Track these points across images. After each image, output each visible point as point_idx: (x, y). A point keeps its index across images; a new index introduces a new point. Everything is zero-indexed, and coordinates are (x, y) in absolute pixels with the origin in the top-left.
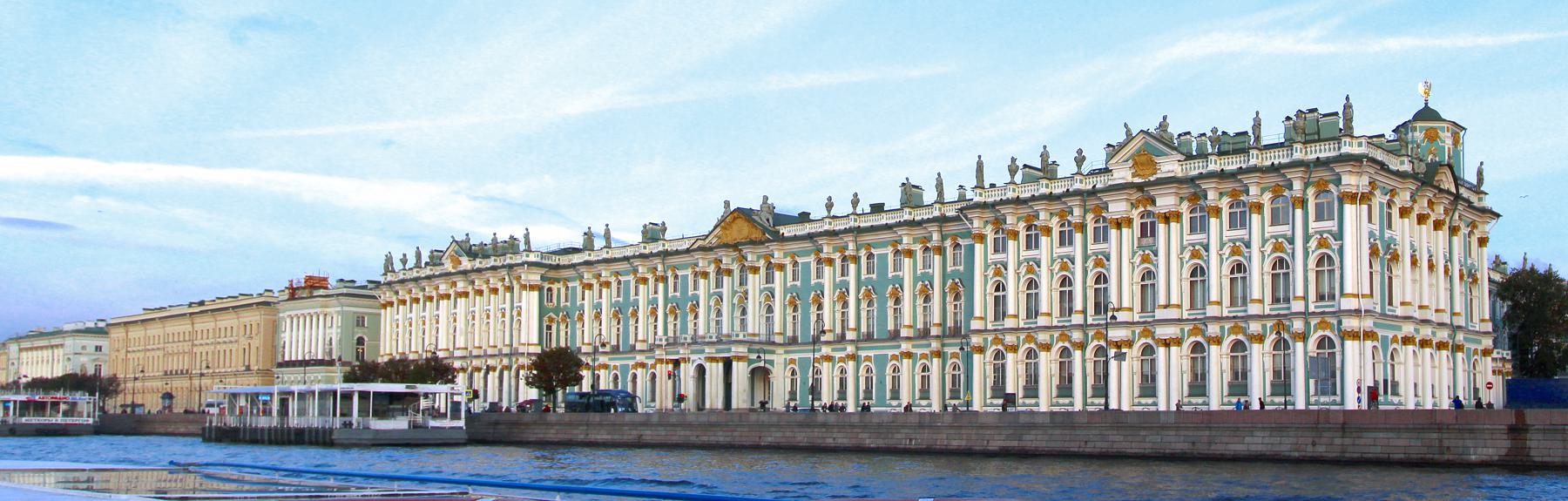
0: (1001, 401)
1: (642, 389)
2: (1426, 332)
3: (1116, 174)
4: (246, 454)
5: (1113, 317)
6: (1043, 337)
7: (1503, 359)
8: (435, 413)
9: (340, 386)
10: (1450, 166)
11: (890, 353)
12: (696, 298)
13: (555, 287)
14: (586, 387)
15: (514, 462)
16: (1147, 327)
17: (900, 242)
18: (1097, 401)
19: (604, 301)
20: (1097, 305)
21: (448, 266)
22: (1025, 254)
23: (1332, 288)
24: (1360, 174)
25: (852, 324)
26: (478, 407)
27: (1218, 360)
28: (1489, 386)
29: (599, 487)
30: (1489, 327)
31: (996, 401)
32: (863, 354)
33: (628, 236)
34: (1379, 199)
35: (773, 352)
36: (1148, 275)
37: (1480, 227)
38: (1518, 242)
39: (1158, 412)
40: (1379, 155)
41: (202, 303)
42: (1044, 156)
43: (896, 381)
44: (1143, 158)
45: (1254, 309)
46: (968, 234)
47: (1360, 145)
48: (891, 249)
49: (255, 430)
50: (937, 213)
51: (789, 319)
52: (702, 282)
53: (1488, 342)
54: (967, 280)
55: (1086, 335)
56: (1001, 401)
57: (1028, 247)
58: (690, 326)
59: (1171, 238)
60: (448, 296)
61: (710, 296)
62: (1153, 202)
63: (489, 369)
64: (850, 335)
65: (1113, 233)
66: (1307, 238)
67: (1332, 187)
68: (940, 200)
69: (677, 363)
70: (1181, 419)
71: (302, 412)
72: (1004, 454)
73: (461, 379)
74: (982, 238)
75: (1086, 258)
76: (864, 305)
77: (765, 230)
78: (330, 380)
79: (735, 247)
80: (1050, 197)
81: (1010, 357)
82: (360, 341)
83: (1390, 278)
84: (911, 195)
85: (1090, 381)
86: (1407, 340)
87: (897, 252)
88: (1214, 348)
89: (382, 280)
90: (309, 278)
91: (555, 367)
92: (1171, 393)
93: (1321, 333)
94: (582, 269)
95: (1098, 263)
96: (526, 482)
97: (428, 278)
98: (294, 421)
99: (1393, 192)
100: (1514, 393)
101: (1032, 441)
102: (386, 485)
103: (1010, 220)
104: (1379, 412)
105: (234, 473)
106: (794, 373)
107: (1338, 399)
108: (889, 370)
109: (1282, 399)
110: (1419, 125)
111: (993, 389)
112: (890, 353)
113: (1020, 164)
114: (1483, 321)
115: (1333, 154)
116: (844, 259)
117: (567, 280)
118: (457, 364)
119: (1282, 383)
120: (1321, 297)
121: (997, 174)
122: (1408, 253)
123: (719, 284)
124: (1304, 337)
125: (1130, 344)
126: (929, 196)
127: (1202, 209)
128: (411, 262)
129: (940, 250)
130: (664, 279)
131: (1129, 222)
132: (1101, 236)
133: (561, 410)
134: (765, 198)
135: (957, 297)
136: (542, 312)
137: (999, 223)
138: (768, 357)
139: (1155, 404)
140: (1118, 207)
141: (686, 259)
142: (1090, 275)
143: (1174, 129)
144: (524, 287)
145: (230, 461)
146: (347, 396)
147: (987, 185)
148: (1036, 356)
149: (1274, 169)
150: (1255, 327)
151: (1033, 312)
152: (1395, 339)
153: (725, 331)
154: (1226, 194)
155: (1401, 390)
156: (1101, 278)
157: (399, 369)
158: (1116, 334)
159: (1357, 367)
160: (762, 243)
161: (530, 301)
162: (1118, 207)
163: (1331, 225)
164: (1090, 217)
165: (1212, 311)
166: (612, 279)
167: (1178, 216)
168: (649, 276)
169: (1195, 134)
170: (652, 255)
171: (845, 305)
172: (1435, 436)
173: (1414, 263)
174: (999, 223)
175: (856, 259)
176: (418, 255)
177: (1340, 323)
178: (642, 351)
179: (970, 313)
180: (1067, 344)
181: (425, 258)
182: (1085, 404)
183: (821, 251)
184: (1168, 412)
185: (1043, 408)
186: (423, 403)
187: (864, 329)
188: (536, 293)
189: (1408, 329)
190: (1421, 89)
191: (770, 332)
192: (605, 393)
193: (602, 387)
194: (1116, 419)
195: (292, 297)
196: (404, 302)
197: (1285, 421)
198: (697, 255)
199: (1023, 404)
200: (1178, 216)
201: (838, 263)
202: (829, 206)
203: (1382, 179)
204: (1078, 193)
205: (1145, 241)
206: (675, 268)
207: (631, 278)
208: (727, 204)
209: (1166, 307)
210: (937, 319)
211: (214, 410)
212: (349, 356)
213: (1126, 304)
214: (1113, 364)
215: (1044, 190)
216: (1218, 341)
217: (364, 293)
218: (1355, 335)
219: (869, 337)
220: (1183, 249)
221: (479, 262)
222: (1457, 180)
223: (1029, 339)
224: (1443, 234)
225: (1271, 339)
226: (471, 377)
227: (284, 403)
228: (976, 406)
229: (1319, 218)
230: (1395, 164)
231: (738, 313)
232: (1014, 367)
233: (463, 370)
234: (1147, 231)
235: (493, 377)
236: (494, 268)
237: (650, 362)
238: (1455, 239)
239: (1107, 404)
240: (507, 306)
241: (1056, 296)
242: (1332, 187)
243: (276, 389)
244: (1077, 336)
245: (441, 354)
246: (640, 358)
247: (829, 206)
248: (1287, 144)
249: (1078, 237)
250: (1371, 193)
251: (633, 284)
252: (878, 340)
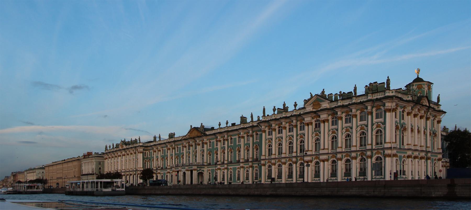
0: (270, 180)
1: (169, 179)
2: (416, 153)
3: (307, 109)
4: (75, 198)
5: (306, 153)
6: (283, 160)
7: (446, 162)
8: (118, 187)
9: (95, 180)
10: (427, 97)
11: (237, 167)
12: (183, 153)
13: (147, 152)
14: (155, 179)
15: (138, 200)
16: (317, 156)
17: (240, 134)
18: (300, 179)
19: (159, 155)
21: (120, 148)
22: (278, 135)
23: (381, 141)
24: (392, 102)
25: (226, 159)
26: (128, 185)
27: (341, 166)
28: (440, 171)
29: (158, 206)
30: (441, 151)
31: (269, 180)
32: (229, 167)
33: (165, 137)
34: (399, 110)
35: (204, 168)
36: (318, 139)
37: (438, 117)
38: (450, 122)
39: (320, 182)
40: (400, 95)
41: (64, 160)
42: (284, 105)
43: (239, 175)
44: (316, 103)
45: (353, 149)
46: (261, 130)
47: (392, 92)
48: (237, 136)
49: (77, 192)
50: (251, 125)
51: (208, 158)
52: (184, 149)
53: (440, 156)
54: (260, 144)
55: (297, 159)
56: (270, 180)
57: (279, 133)
58: (182, 161)
59: (325, 128)
60: (120, 156)
61: (187, 152)
62: (320, 117)
63: (131, 175)
64: (226, 162)
65: (306, 127)
66: (372, 125)
67: (382, 107)
68: (252, 121)
70: (328, 184)
71: (87, 187)
72: (271, 196)
73: (124, 177)
74: (265, 131)
75: (297, 135)
76: (230, 153)
77: (202, 133)
78: (93, 179)
79: (193, 138)
80: (286, 118)
81: (273, 167)
82: (100, 168)
83: (403, 136)
84: (243, 120)
85: (298, 173)
86: (409, 157)
87: (239, 137)
88: (339, 162)
89: (104, 152)
90: (88, 153)
91: (147, 173)
92: (325, 176)
93: (377, 155)
94: (153, 147)
95: (301, 137)
96: (140, 205)
97: (116, 151)
98: (85, 189)
99: (404, 107)
100: (449, 173)
101: (280, 192)
102: (106, 205)
103: (273, 125)
104: (397, 182)
105: (72, 202)
106: (210, 173)
107: (383, 177)
108: (237, 172)
109: (363, 177)
110: (415, 84)
111: (268, 176)
112: (237, 167)
113: (276, 108)
114: (438, 149)
115: (382, 96)
116: (224, 140)
117: (150, 150)
118: (123, 174)
119: (363, 172)
120: (377, 144)
121: (269, 112)
122: (410, 127)
123: (189, 149)
124: (371, 157)
125: (311, 161)
126: (249, 120)
127: (336, 118)
128: (111, 147)
129: (252, 136)
130: (175, 148)
132: (302, 128)
133: (148, 185)
134: (202, 124)
135: (257, 150)
137: (270, 126)
138: (203, 169)
139: (319, 180)
140: (307, 119)
141: (180, 142)
142: (298, 141)
143: (327, 93)
144: (139, 152)
145: (71, 200)
146: (97, 183)
147: (266, 115)
148: (281, 166)
149: (361, 103)
150: (353, 155)
151: (280, 152)
152: (404, 157)
153: (191, 162)
154: (344, 112)
155: (406, 173)
156: (302, 142)
157: (109, 175)
158: (306, 159)
159: (390, 166)
160: (201, 137)
161: (140, 156)
162: (307, 119)
163: (382, 120)
164: (298, 123)
165: (339, 150)
166: (161, 149)
167: (328, 121)
168: (171, 148)
169: (334, 94)
170: (171, 142)
171: (224, 153)
172: (419, 188)
173: (412, 130)
174: (270, 126)
175: (227, 140)
176: (113, 145)
177: (384, 152)
178: (169, 169)
179: (261, 154)
180: (291, 162)
181: (115, 146)
182: (297, 180)
183: (217, 138)
184: (324, 182)
185: (283, 182)
186: (115, 184)
187: (229, 160)
188: (142, 154)
189: (409, 153)
190: (416, 71)
191: (203, 162)
192: (160, 180)
193: (159, 179)
194: (307, 184)
195: (84, 158)
196: (110, 158)
197: (364, 184)
198: (183, 141)
199: (277, 181)
200: (328, 121)
201: (222, 141)
202: (220, 125)
203: (401, 103)
204: (295, 115)
205: (316, 129)
206: (178, 145)
207: (166, 148)
208: (191, 126)
209: (323, 149)
210: (251, 156)
211: (68, 187)
212: (97, 173)
213: (310, 149)
214: (306, 168)
215: (284, 116)
216: (341, 159)
217: (100, 156)
218: (389, 156)
219: (231, 162)
220: (329, 131)
221: (128, 146)
222: (430, 101)
223: (279, 161)
224: (423, 121)
225: (359, 158)
226: (126, 177)
227: (83, 185)
228: (263, 182)
229: (377, 118)
230: (405, 98)
231: (194, 157)
232: (274, 170)
233: (124, 175)
235: (131, 177)
236: (131, 148)
237: (171, 172)
238: (428, 122)
239: (304, 180)
240: (135, 158)
241: (288, 148)
243: (81, 181)
244: (294, 160)
245: (119, 171)
246: (168, 170)
247: (220, 125)
248: (366, 94)
249: (295, 129)
250: (396, 108)
251: (166, 150)
252: (234, 163)
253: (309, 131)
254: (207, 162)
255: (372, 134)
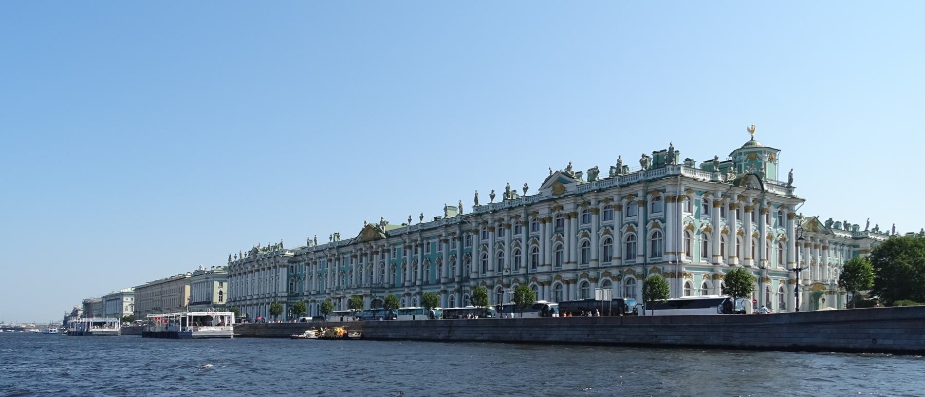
11: (437, 291)
20: (534, 263)
25: (419, 277)
59: (570, 227)
60: (251, 272)
62: (562, 208)
64: (418, 283)
66: (646, 222)
69: (340, 299)
75: (528, 239)
112: (437, 291)
131: (550, 219)
136: (288, 277)
142: (530, 248)
156: (535, 250)
161: (283, 272)
167: (576, 215)
187: (425, 279)
200: (576, 215)
205: (559, 229)
210: (457, 273)
234: (559, 224)
242: (661, 193)
253: (545, 232)
254: (389, 283)
255: (645, 237)
